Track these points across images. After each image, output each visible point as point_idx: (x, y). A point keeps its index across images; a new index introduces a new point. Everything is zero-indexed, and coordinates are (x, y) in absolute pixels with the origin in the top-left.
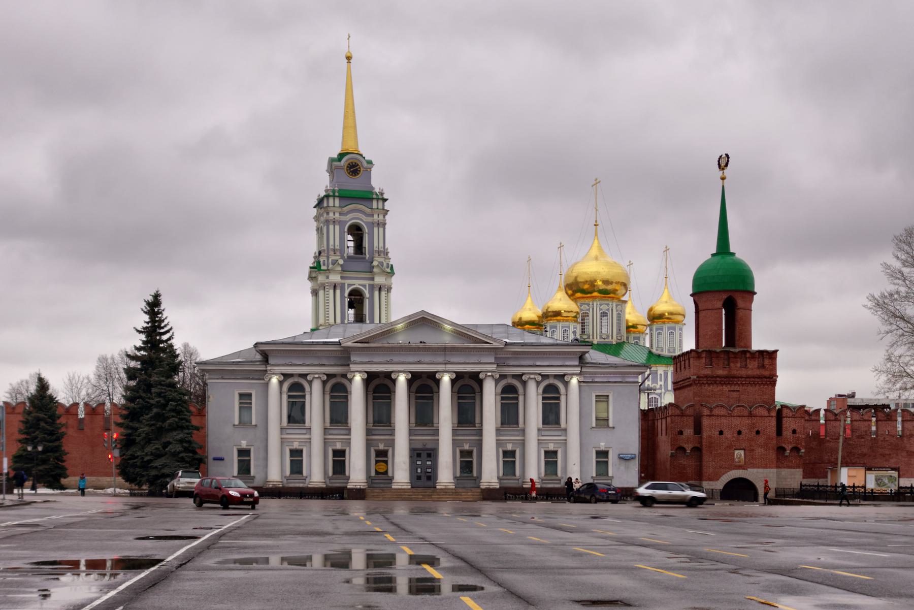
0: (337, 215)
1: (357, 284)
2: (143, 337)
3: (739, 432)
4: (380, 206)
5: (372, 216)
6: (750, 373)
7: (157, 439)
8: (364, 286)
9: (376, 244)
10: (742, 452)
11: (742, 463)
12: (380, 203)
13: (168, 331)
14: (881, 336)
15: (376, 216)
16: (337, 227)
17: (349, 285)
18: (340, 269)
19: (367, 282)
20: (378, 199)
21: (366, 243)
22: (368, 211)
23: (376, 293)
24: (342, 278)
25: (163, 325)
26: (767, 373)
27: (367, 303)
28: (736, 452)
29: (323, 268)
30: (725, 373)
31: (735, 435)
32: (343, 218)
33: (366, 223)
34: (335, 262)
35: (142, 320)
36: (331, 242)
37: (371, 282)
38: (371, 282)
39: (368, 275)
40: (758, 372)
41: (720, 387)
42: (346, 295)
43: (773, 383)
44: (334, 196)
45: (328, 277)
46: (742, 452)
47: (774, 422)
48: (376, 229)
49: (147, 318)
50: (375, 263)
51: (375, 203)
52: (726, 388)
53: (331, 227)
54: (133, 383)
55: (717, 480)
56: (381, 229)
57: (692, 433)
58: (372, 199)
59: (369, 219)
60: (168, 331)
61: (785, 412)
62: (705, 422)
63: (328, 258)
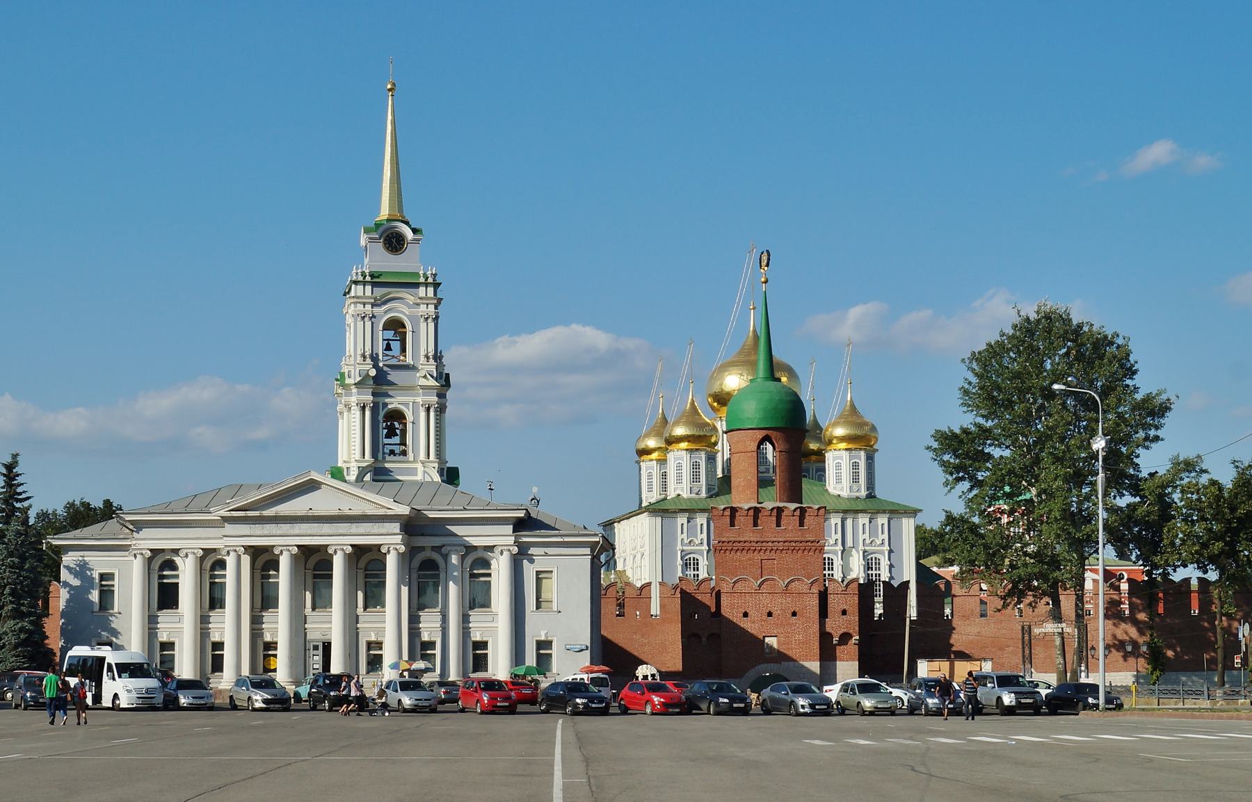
0: (368, 307)
3: (770, 614)
8: (406, 405)
13: (28, 498)
16: (368, 324)
23: (423, 415)
27: (409, 427)
31: (765, 617)
41: (750, 555)
42: (381, 418)
44: (364, 283)
47: (814, 602)
48: (423, 325)
52: (757, 556)
55: (741, 676)
60: (28, 498)
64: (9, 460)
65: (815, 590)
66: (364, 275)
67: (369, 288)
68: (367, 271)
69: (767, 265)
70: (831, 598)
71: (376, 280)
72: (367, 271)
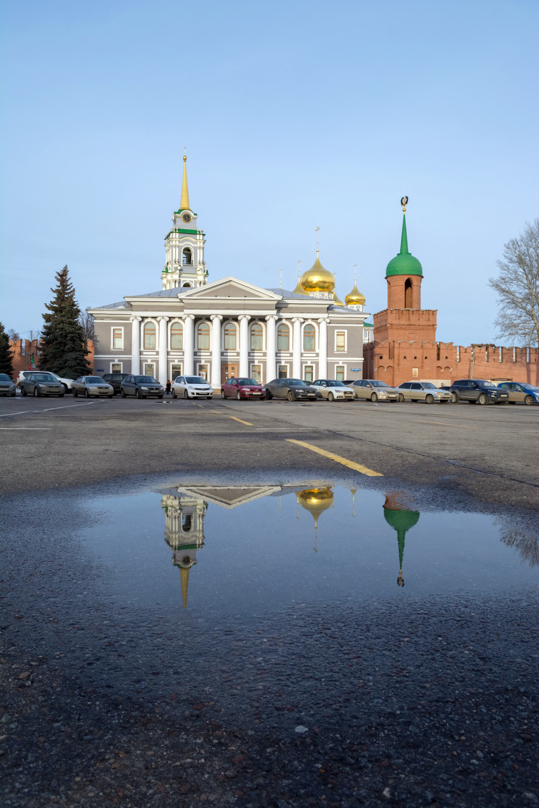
0: (177, 242)
1: (188, 280)
2: (55, 295)
4: (201, 238)
5: (196, 243)
6: (421, 323)
7: (61, 357)
8: (192, 282)
9: (198, 259)
10: (417, 369)
11: (417, 376)
12: (201, 236)
14: (498, 303)
15: (198, 243)
16: (177, 249)
17: (184, 281)
18: (178, 272)
19: (193, 280)
20: (200, 234)
21: (193, 258)
22: (194, 240)
24: (179, 277)
25: (68, 288)
26: (431, 323)
28: (414, 369)
29: (169, 271)
30: (407, 323)
32: (180, 244)
33: (193, 247)
34: (176, 269)
35: (56, 284)
36: (174, 257)
37: (196, 280)
38: (196, 280)
39: (195, 276)
40: (425, 323)
43: (435, 330)
44: (176, 232)
45: (172, 277)
46: (417, 369)
47: (435, 353)
48: (198, 251)
49: (58, 283)
50: (198, 269)
51: (198, 236)
52: (407, 332)
53: (174, 249)
54: (49, 324)
56: (201, 251)
57: (388, 358)
58: (197, 234)
59: (195, 245)
61: (442, 347)
62: (396, 352)
63: (172, 265)
64: (60, 270)
65: (436, 347)
66: (176, 230)
67: (177, 234)
68: (177, 229)
69: (406, 203)
70: (441, 351)
71: (181, 232)
72: (177, 229)
